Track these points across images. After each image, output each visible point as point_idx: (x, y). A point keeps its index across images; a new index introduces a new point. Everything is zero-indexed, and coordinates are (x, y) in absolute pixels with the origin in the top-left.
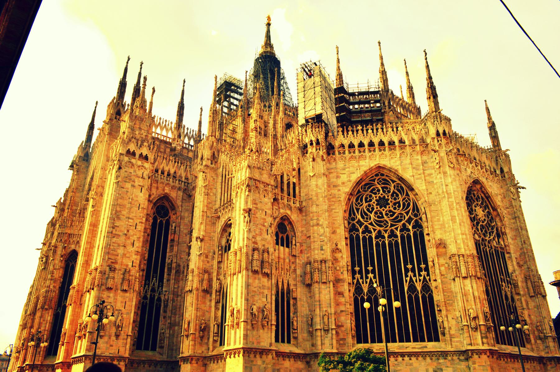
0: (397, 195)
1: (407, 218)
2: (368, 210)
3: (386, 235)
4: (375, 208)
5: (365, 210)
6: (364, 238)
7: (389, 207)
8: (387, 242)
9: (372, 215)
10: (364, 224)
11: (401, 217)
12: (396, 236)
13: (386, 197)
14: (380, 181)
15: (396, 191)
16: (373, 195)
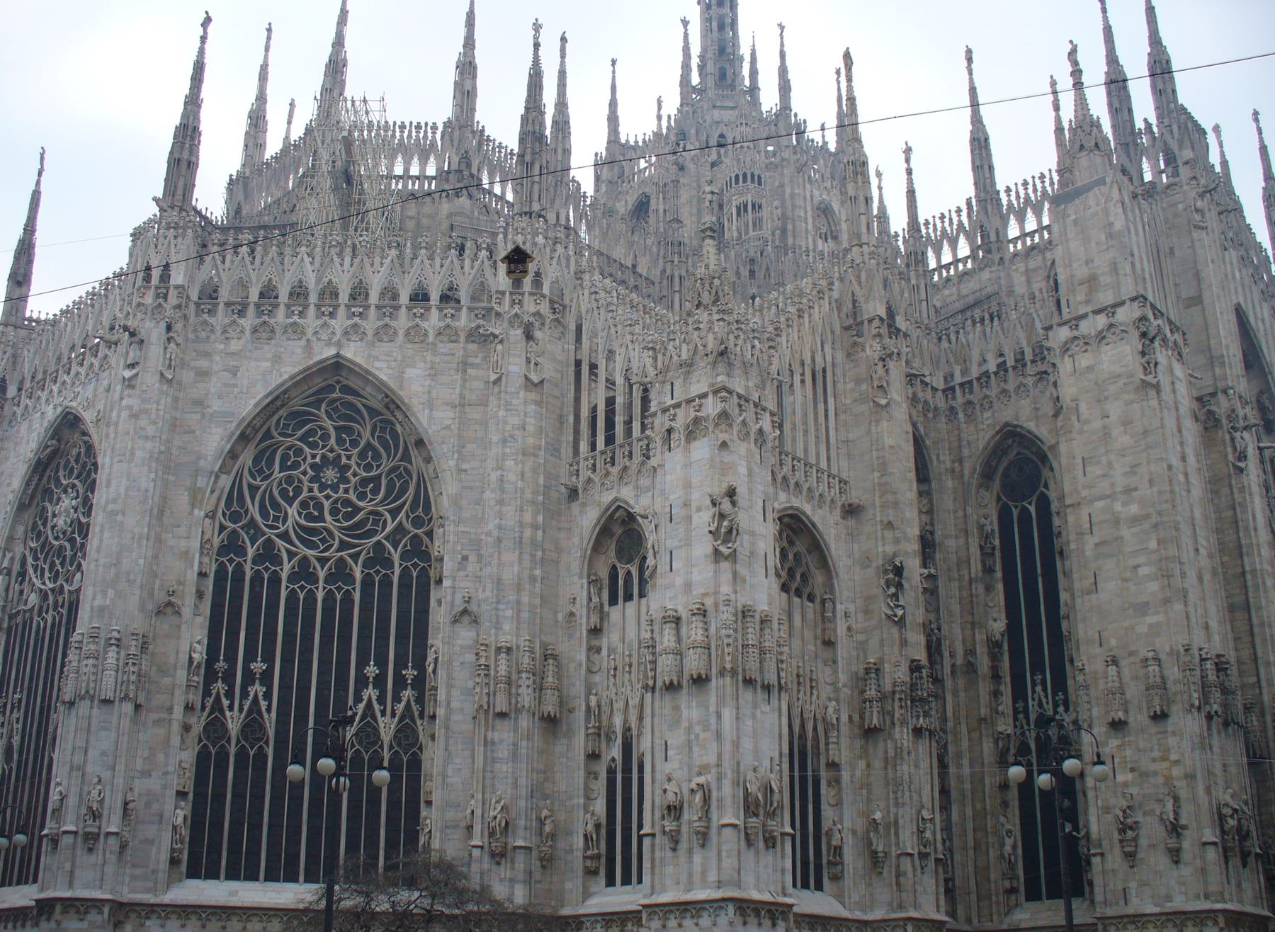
0: (377, 456)
1: (389, 528)
2: (283, 493)
3: (322, 575)
4: (305, 489)
5: (276, 493)
6: (257, 578)
7: (346, 491)
8: (320, 595)
9: (292, 511)
10: (264, 534)
11: (376, 522)
12: (350, 579)
13: (344, 460)
14: (336, 410)
15: (376, 444)
16: (307, 450)
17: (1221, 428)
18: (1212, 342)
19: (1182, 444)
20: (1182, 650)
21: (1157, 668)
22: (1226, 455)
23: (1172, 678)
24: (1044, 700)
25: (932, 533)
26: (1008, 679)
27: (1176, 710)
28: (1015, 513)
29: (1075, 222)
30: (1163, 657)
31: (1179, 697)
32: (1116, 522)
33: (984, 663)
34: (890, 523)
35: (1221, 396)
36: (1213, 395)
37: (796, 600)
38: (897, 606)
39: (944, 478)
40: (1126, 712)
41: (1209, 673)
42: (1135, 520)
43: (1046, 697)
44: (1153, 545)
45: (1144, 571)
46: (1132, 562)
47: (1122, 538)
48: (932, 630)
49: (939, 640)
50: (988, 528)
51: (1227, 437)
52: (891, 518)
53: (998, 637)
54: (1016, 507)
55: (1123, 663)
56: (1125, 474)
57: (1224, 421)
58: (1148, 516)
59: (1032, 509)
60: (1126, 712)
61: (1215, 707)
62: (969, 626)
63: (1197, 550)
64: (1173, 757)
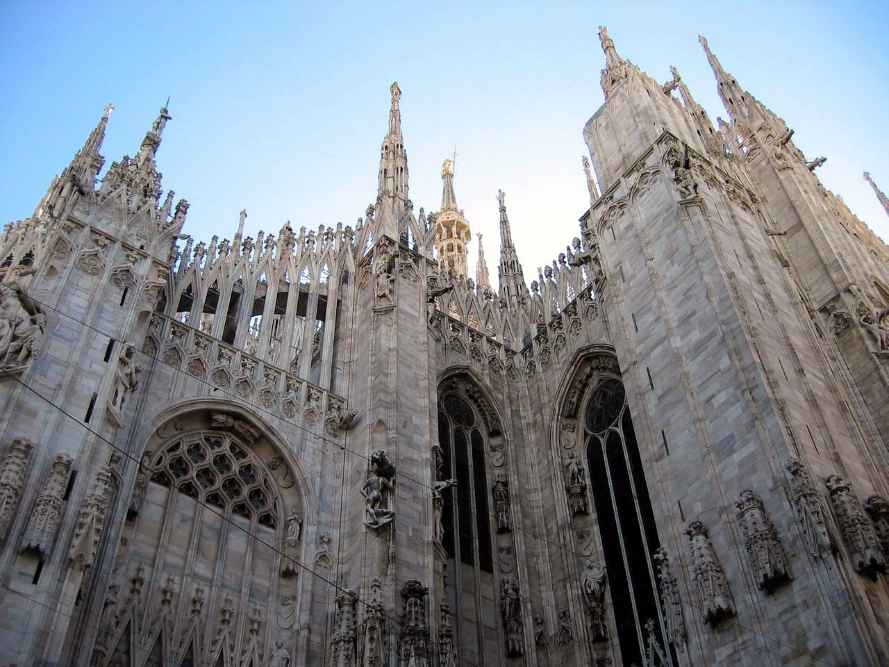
17: (854, 325)
18: (822, 253)
19: (755, 268)
20: (789, 476)
21: (757, 513)
22: (867, 349)
23: (784, 522)
24: (660, 653)
25: (505, 485)
26: (616, 640)
27: (800, 568)
28: (603, 442)
29: (607, 127)
30: (765, 497)
31: (799, 543)
32: (677, 358)
33: (580, 624)
34: (380, 422)
35: (846, 298)
36: (837, 298)
37: (239, 519)
38: (378, 514)
39: (525, 433)
40: (729, 596)
41: (848, 506)
42: (698, 347)
43: (662, 647)
44: (725, 362)
45: (721, 398)
46: (703, 397)
47: (686, 374)
48: (506, 592)
49: (516, 604)
50: (574, 467)
51: (863, 331)
52: (381, 417)
53: (595, 586)
54: (603, 436)
55: (713, 531)
56: (679, 306)
57: (854, 317)
58: (713, 334)
59: (620, 430)
60: (729, 596)
61: (869, 553)
62: (561, 584)
63: (801, 371)
64: (813, 644)
